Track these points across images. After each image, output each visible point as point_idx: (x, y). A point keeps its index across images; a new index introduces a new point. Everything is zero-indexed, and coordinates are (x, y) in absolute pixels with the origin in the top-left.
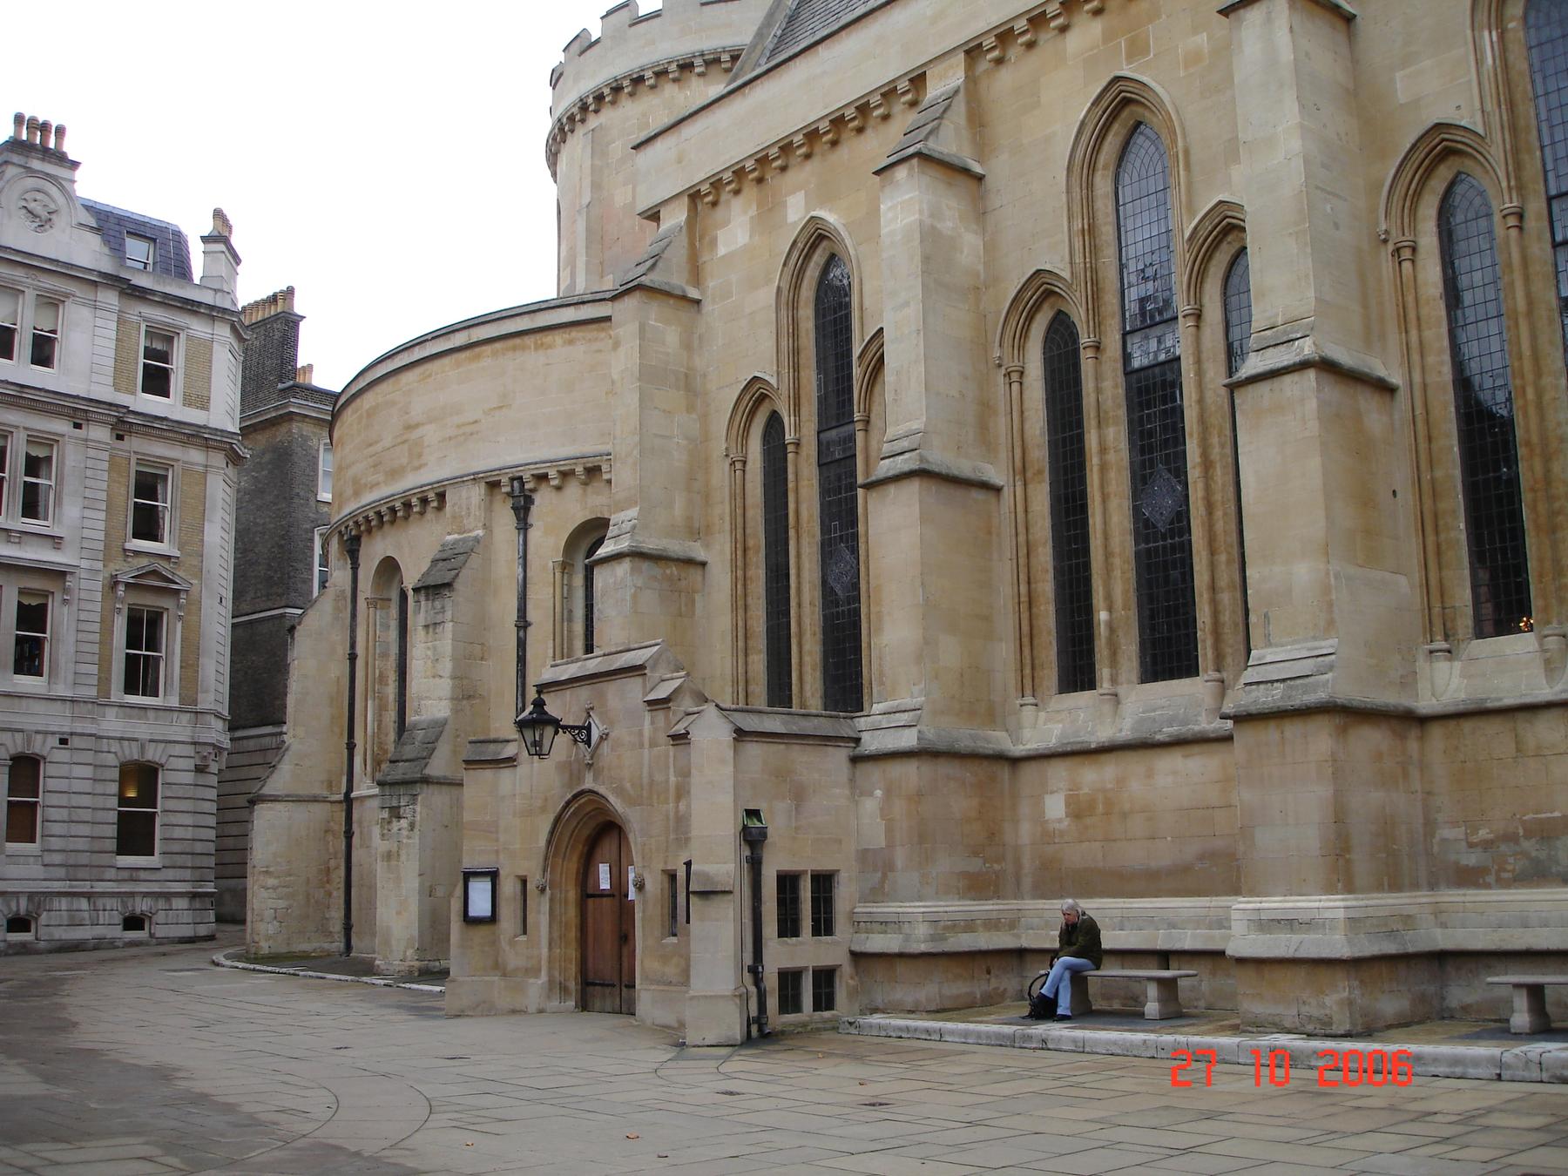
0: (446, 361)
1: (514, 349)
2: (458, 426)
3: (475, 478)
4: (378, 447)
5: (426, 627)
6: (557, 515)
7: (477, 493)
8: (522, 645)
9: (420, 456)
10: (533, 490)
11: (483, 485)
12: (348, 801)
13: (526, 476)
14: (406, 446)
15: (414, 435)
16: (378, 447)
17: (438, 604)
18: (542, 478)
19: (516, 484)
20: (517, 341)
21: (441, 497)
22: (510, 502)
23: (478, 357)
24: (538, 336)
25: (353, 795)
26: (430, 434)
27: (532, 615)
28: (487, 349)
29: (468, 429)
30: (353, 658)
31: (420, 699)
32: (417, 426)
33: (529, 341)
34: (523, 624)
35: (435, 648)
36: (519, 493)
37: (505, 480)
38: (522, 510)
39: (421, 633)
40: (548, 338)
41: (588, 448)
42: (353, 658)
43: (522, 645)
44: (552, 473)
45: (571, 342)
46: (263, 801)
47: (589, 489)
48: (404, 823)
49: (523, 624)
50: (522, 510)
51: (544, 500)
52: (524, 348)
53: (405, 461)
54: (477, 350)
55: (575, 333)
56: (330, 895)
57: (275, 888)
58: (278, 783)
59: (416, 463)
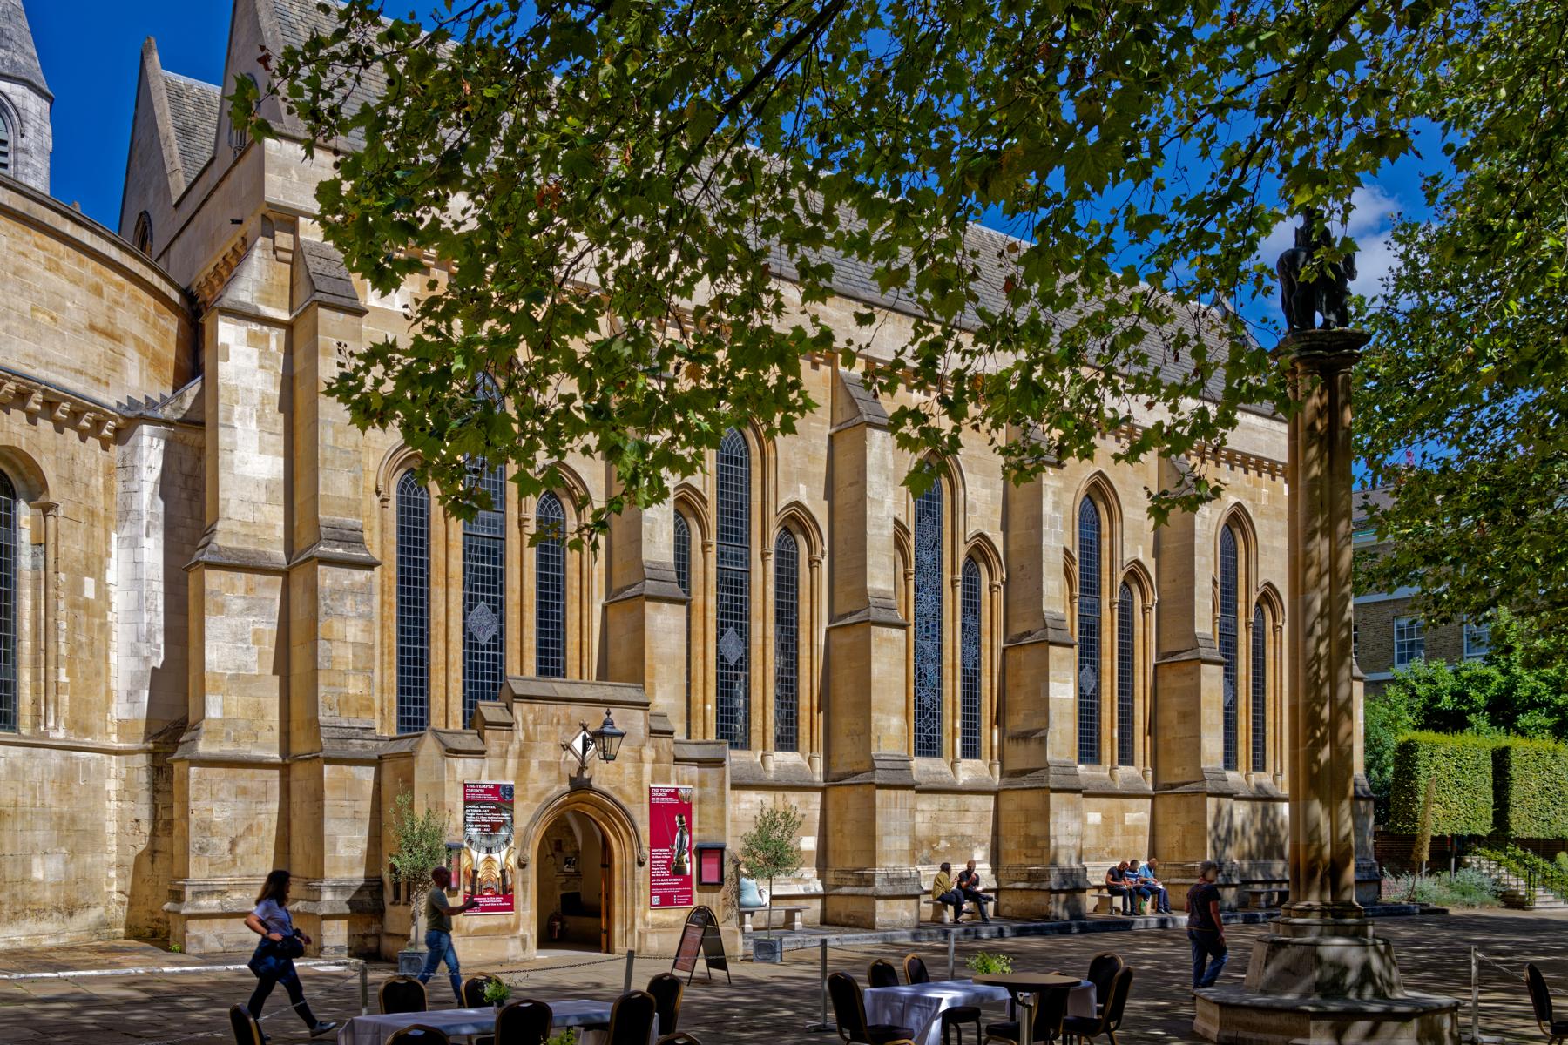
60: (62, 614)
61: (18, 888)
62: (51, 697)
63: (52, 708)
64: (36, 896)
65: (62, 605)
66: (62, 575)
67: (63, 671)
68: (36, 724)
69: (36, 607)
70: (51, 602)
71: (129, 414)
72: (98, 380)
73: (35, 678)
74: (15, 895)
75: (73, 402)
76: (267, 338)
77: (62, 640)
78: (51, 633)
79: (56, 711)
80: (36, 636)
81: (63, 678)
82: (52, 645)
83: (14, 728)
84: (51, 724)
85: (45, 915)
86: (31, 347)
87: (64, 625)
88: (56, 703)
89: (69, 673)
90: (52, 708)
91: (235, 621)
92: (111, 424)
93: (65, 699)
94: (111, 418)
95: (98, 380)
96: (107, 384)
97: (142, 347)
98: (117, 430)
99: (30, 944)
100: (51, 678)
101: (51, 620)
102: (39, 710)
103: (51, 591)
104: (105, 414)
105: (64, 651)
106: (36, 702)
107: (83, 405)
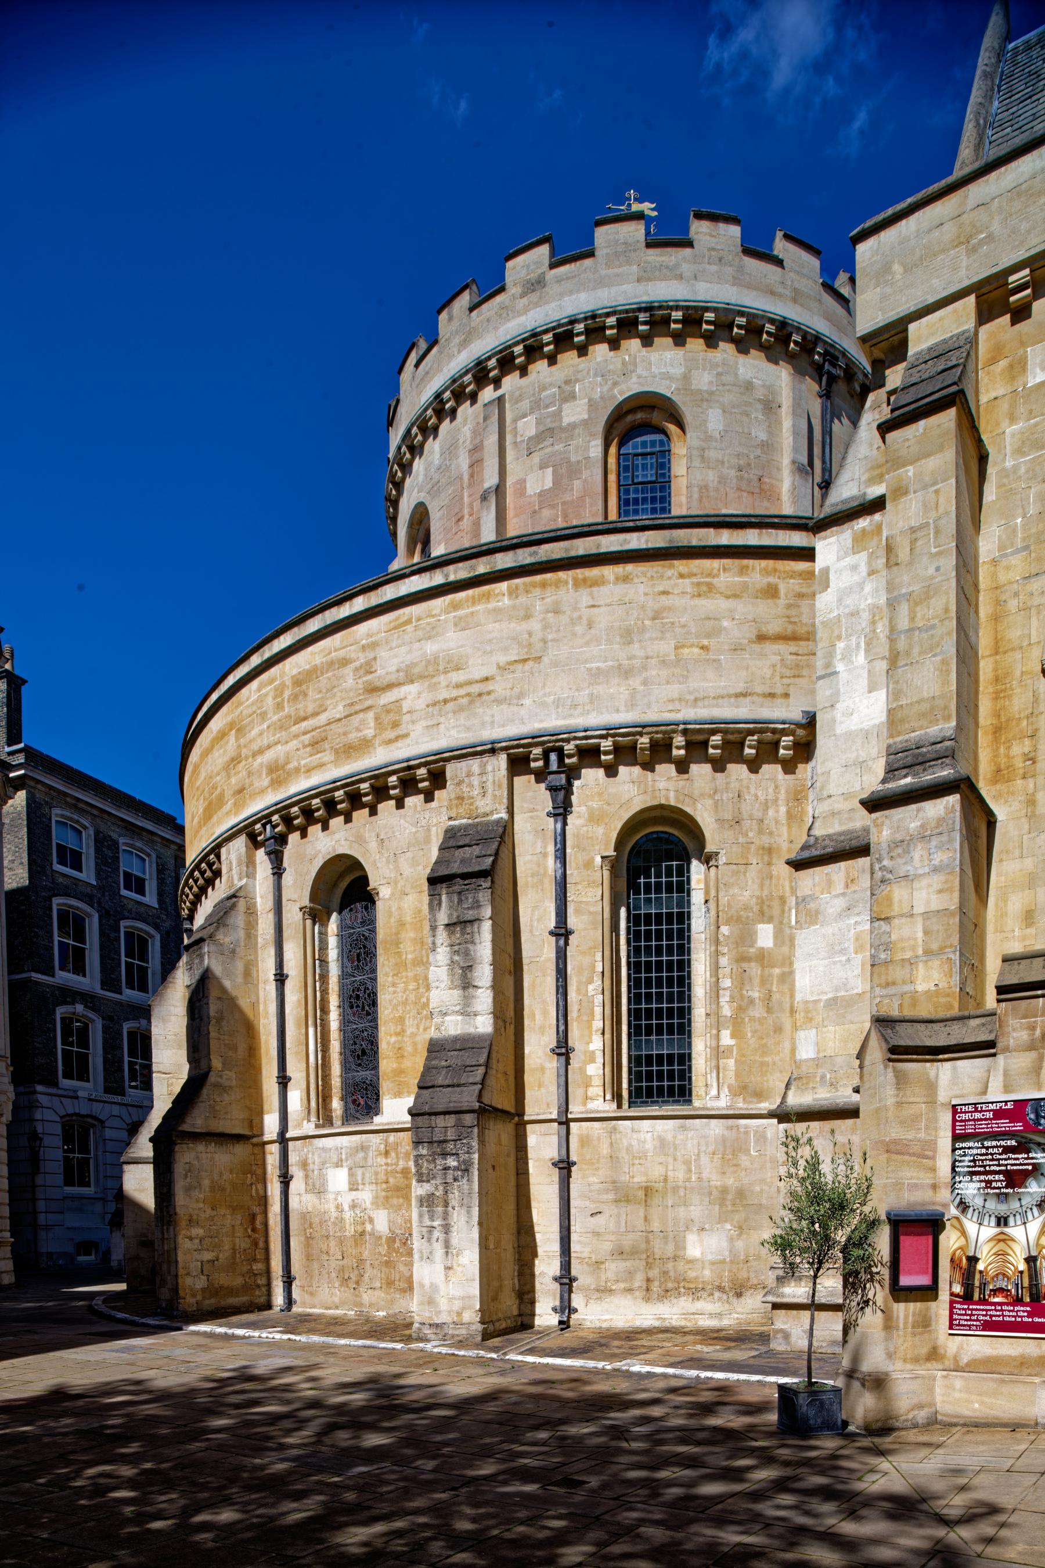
4: (323, 718)
9: (396, 725)
11: (503, 758)
13: (569, 748)
14: (371, 715)
16: (323, 718)
19: (553, 757)
26: (412, 696)
32: (390, 686)
35: (467, 953)
37: (537, 751)
39: (442, 935)
41: (653, 716)
48: (452, 1162)
53: (369, 732)
59: (391, 734)
61: (670, 1265)
64: (692, 1274)
72: (772, 695)
74: (665, 1273)
75: (725, 732)
85: (704, 1294)
86: (674, 690)
91: (829, 930)
92: (786, 740)
94: (784, 732)
95: (772, 695)
96: (786, 695)
98: (796, 745)
99: (683, 1323)
104: (774, 731)
107: (739, 731)
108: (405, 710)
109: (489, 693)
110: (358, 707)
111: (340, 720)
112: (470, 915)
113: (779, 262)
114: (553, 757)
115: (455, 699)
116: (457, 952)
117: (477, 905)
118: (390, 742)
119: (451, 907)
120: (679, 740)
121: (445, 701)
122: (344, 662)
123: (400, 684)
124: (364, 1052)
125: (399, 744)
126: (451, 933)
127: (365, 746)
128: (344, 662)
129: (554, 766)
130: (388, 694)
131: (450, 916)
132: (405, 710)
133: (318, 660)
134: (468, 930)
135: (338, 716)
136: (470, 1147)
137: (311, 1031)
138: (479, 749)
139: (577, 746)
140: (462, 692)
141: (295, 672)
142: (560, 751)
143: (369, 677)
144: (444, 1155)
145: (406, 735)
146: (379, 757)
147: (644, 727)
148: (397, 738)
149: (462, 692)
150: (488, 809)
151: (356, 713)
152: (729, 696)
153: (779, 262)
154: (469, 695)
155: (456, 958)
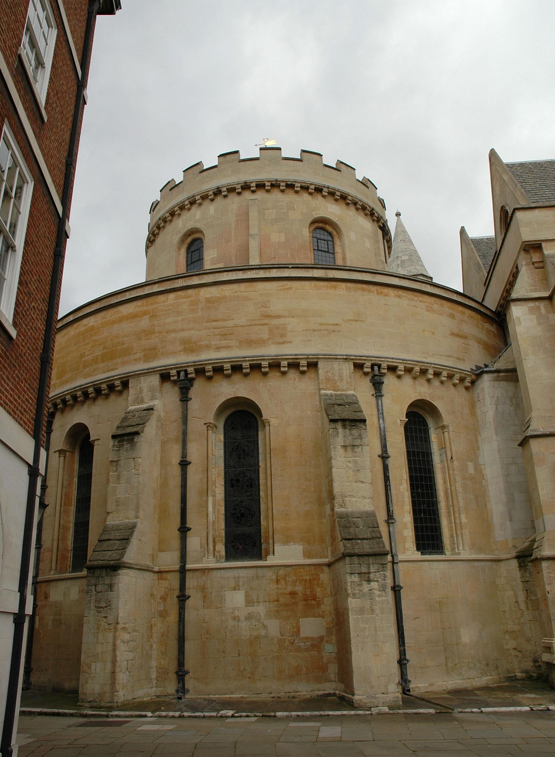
0: (307, 283)
1: (363, 290)
2: (320, 324)
3: (347, 359)
4: (230, 323)
5: (345, 447)
6: (400, 395)
7: (348, 368)
8: (386, 468)
9: (283, 336)
10: (383, 375)
12: (183, 571)
13: (384, 365)
14: (266, 328)
15: (275, 322)
17: (355, 432)
18: (392, 369)
19: (376, 368)
20: (365, 286)
21: (313, 365)
22: (368, 379)
23: (335, 288)
24: (379, 288)
25: (188, 566)
27: (390, 451)
28: (343, 285)
29: (331, 328)
30: (184, 464)
31: (343, 496)
32: (278, 317)
33: (372, 288)
34: (384, 457)
35: (356, 462)
36: (375, 373)
37: (368, 364)
38: (377, 385)
39: (341, 451)
40: (386, 290)
42: (184, 464)
43: (386, 468)
44: (401, 367)
45: (399, 297)
46: (125, 567)
47: (417, 382)
49: (384, 457)
50: (377, 385)
51: (389, 381)
52: (369, 291)
53: (266, 337)
54: (334, 283)
55: (401, 292)
56: (152, 646)
57: (128, 642)
58: (131, 555)
59: (281, 341)
60: (458, 485)
62: (459, 532)
63: (460, 538)
65: (458, 479)
66: (455, 463)
67: (463, 516)
68: (453, 549)
69: (445, 482)
70: (452, 478)
71: (476, 372)
73: (450, 522)
76: (539, 307)
77: (460, 498)
78: (454, 495)
79: (462, 540)
80: (447, 498)
81: (464, 520)
82: (455, 502)
83: (442, 553)
84: (461, 547)
87: (460, 489)
88: (462, 534)
89: (466, 518)
90: (460, 538)
93: (466, 532)
97: (479, 341)
100: (458, 521)
101: (453, 488)
102: (453, 540)
103: (451, 472)
105: (461, 504)
106: (452, 536)
108: (289, 330)
109: (339, 331)
110: (257, 322)
111: (243, 326)
112: (358, 442)
113: (368, 188)
114: (376, 368)
115: (320, 330)
116: (349, 462)
117: (360, 437)
118: (279, 343)
119: (345, 436)
120: (431, 371)
121: (314, 330)
122: (247, 299)
123: (285, 317)
124: (243, 515)
125: (286, 345)
126: (346, 451)
127: (261, 342)
128: (247, 299)
129: (377, 372)
130: (277, 320)
131: (344, 441)
132: (289, 330)
133: (227, 293)
134: (356, 450)
135: (242, 324)
136: (385, 576)
137: (210, 499)
138: (339, 357)
139: (387, 365)
140: (324, 327)
141: (208, 296)
142: (379, 366)
143: (264, 309)
144: (369, 581)
145: (291, 342)
146: (271, 351)
147: (418, 362)
148: (284, 343)
149: (324, 327)
150: (345, 388)
151: (256, 325)
152: (445, 356)
153: (368, 188)
154: (327, 330)
155: (349, 464)
